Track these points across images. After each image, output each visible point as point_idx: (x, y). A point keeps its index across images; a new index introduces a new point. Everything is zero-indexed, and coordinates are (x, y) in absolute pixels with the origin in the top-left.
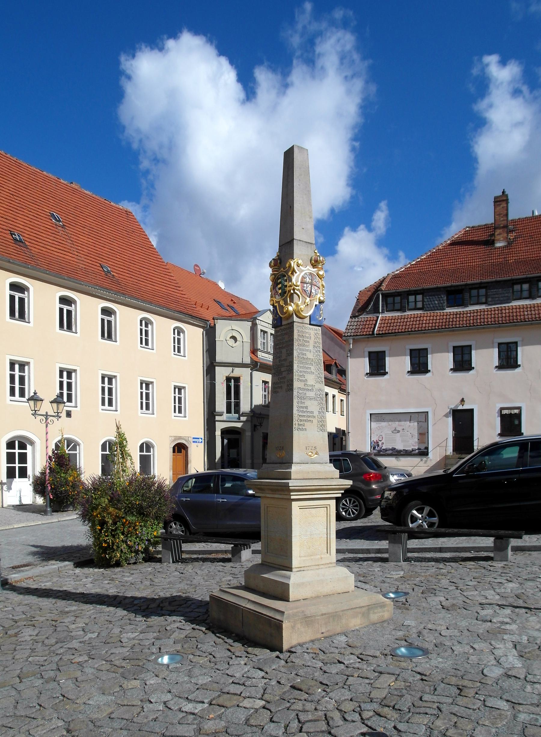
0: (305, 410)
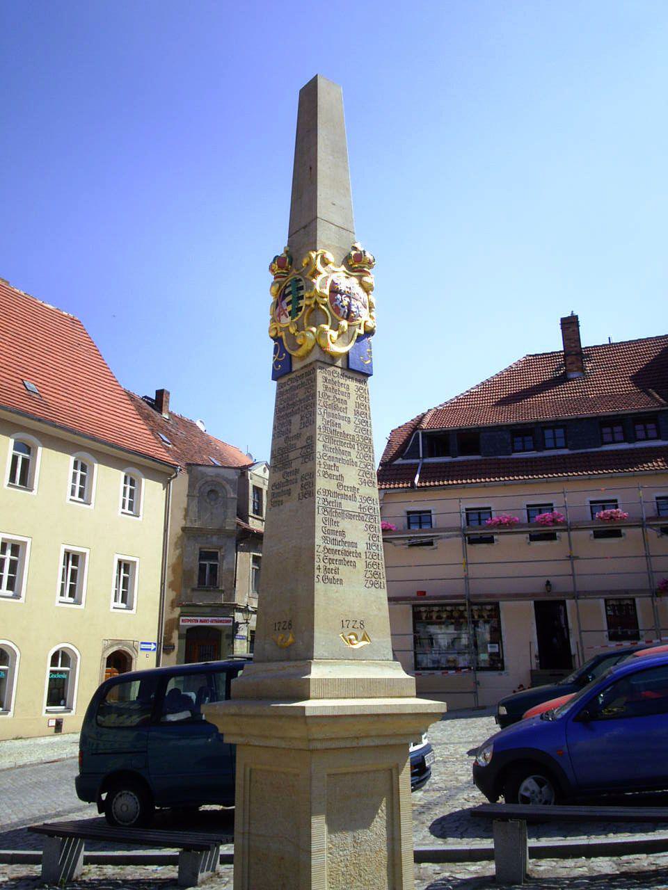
0: (339, 538)
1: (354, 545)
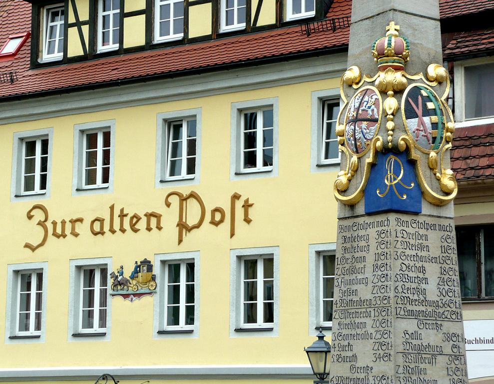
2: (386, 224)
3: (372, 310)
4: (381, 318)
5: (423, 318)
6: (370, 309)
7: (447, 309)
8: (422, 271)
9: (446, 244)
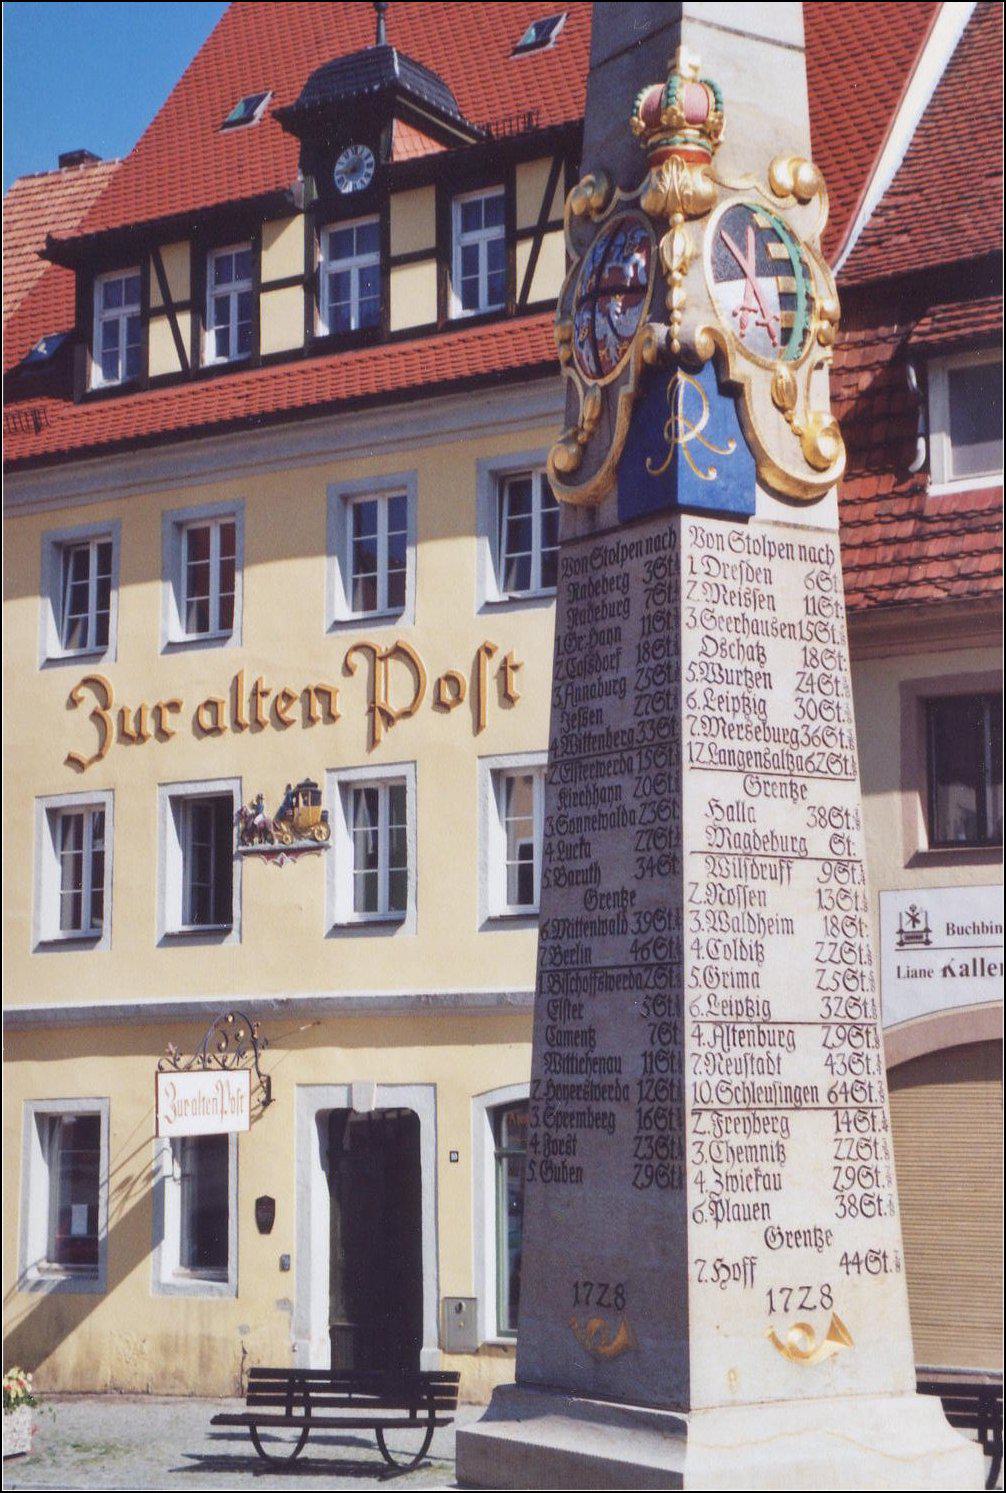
0: (580, 1052)
1: (613, 1064)
2: (666, 544)
3: (633, 754)
4: (654, 772)
5: (759, 770)
6: (631, 753)
7: (817, 750)
8: (756, 657)
9: (817, 593)
